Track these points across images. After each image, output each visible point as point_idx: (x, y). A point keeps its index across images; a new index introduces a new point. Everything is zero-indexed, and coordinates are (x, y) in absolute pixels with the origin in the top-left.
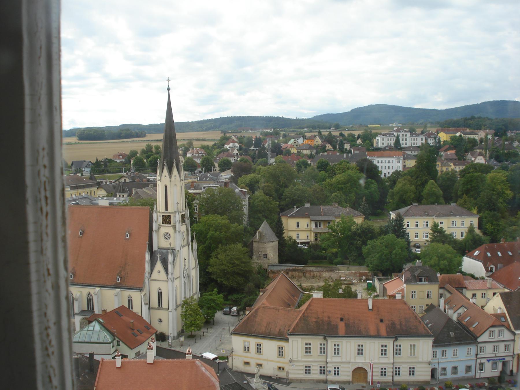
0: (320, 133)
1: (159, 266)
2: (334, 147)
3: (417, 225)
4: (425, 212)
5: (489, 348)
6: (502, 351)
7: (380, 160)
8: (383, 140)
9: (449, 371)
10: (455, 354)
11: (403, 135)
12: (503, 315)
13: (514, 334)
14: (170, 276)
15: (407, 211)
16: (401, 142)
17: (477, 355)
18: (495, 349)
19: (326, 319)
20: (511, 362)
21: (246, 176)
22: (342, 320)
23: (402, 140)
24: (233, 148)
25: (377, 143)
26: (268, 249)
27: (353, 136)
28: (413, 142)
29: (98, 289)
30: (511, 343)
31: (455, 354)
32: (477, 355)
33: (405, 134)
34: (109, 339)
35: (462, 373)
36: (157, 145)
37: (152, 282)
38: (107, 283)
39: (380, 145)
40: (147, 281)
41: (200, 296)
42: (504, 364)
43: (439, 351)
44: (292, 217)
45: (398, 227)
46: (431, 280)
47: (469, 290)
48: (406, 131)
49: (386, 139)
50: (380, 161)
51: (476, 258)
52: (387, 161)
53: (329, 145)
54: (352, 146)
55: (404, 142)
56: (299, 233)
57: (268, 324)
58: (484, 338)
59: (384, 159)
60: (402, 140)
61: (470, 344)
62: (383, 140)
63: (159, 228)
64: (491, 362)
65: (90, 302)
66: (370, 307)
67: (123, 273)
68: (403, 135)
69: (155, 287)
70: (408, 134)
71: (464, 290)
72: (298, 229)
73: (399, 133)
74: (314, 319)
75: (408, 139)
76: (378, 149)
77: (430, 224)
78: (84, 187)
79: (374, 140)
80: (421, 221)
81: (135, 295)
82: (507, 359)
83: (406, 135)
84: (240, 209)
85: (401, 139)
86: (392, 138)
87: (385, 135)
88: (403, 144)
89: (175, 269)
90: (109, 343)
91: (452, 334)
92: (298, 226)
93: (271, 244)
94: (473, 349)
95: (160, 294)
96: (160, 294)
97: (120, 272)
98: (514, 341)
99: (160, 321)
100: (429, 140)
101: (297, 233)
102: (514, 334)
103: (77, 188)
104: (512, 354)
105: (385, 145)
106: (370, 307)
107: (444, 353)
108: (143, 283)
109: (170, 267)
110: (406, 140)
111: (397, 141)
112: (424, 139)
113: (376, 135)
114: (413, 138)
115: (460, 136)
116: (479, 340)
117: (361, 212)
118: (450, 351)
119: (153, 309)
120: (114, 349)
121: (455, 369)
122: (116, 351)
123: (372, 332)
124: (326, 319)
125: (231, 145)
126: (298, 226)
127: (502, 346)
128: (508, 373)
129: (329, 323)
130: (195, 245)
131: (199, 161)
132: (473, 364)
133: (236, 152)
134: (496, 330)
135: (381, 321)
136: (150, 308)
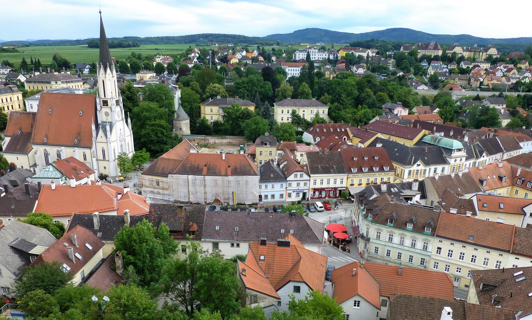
0: (258, 48)
1: (101, 132)
2: (265, 59)
3: (282, 112)
4: (294, 104)
5: (294, 184)
6: (302, 186)
7: (290, 68)
8: (299, 55)
9: (269, 197)
10: (273, 187)
11: (313, 52)
12: (306, 165)
13: (310, 176)
14: (108, 139)
15: (283, 103)
16: (311, 56)
17: (286, 188)
18: (298, 185)
19: (196, 165)
20: (308, 193)
21: (184, 77)
22: (205, 166)
23: (313, 55)
24: (194, 58)
25: (295, 57)
26: (182, 125)
27: (281, 51)
28: (319, 57)
29: (62, 148)
30: (308, 182)
31: (273, 187)
32: (286, 188)
33: (314, 51)
34: (59, 175)
35: (277, 198)
36: (140, 54)
37: (97, 143)
38: (69, 144)
39: (297, 59)
40: (94, 142)
41: (134, 153)
42: (304, 194)
43: (263, 185)
44: (208, 105)
45: (266, 112)
46: (272, 144)
47: (298, 151)
48: (315, 49)
49: (301, 54)
50: (290, 70)
51: (310, 133)
52: (295, 70)
53: (261, 57)
54: (277, 58)
55: (314, 56)
56: (212, 116)
57: (163, 168)
58: (291, 178)
59: (293, 68)
60: (313, 55)
61: (282, 181)
62: (299, 55)
63: (101, 109)
64: (295, 192)
65: (59, 155)
66: (224, 158)
67: (79, 138)
68: (313, 52)
69: (100, 147)
70: (317, 51)
71: (295, 151)
72: (212, 113)
73: (309, 50)
74: (189, 165)
75: (316, 54)
76: (295, 61)
77: (290, 112)
78: (72, 82)
79: (293, 55)
80: (285, 109)
81: (87, 151)
82: (305, 191)
83: (315, 52)
84: (173, 98)
85: (311, 54)
86: (305, 54)
87: (301, 51)
88: (312, 58)
89: (114, 136)
90: (59, 178)
91: (272, 175)
92: (212, 111)
93: (184, 122)
94: (284, 185)
95: (103, 151)
96: (103, 151)
97: (77, 137)
98: (310, 180)
99: (105, 168)
100: (331, 55)
101: (211, 115)
102: (310, 176)
103: (67, 82)
104: (308, 188)
105: (301, 58)
106: (224, 158)
107: (266, 187)
108: (92, 144)
109: (108, 133)
110: (315, 55)
111: (308, 56)
112: (327, 55)
113: (294, 51)
114: (320, 54)
115: (352, 53)
116: (288, 179)
117: (255, 103)
118: (270, 185)
119: (99, 160)
120: (63, 182)
121: (273, 196)
122: (65, 183)
123: (223, 173)
124: (196, 165)
125: (193, 55)
126: (212, 111)
127: (302, 184)
128: (306, 199)
129: (198, 167)
130: (129, 120)
131: (166, 66)
132: (284, 193)
133: (195, 60)
134: (299, 174)
135: (229, 167)
136: (97, 160)
